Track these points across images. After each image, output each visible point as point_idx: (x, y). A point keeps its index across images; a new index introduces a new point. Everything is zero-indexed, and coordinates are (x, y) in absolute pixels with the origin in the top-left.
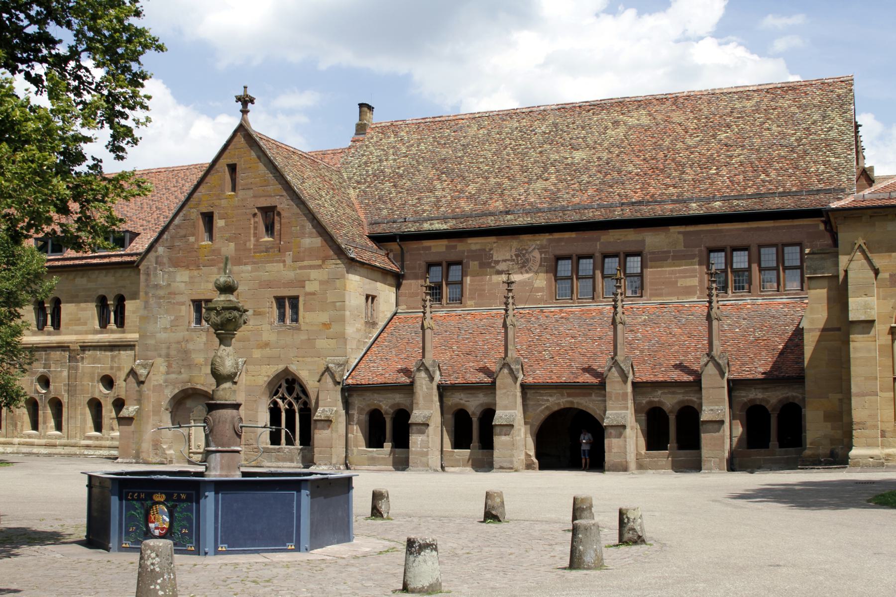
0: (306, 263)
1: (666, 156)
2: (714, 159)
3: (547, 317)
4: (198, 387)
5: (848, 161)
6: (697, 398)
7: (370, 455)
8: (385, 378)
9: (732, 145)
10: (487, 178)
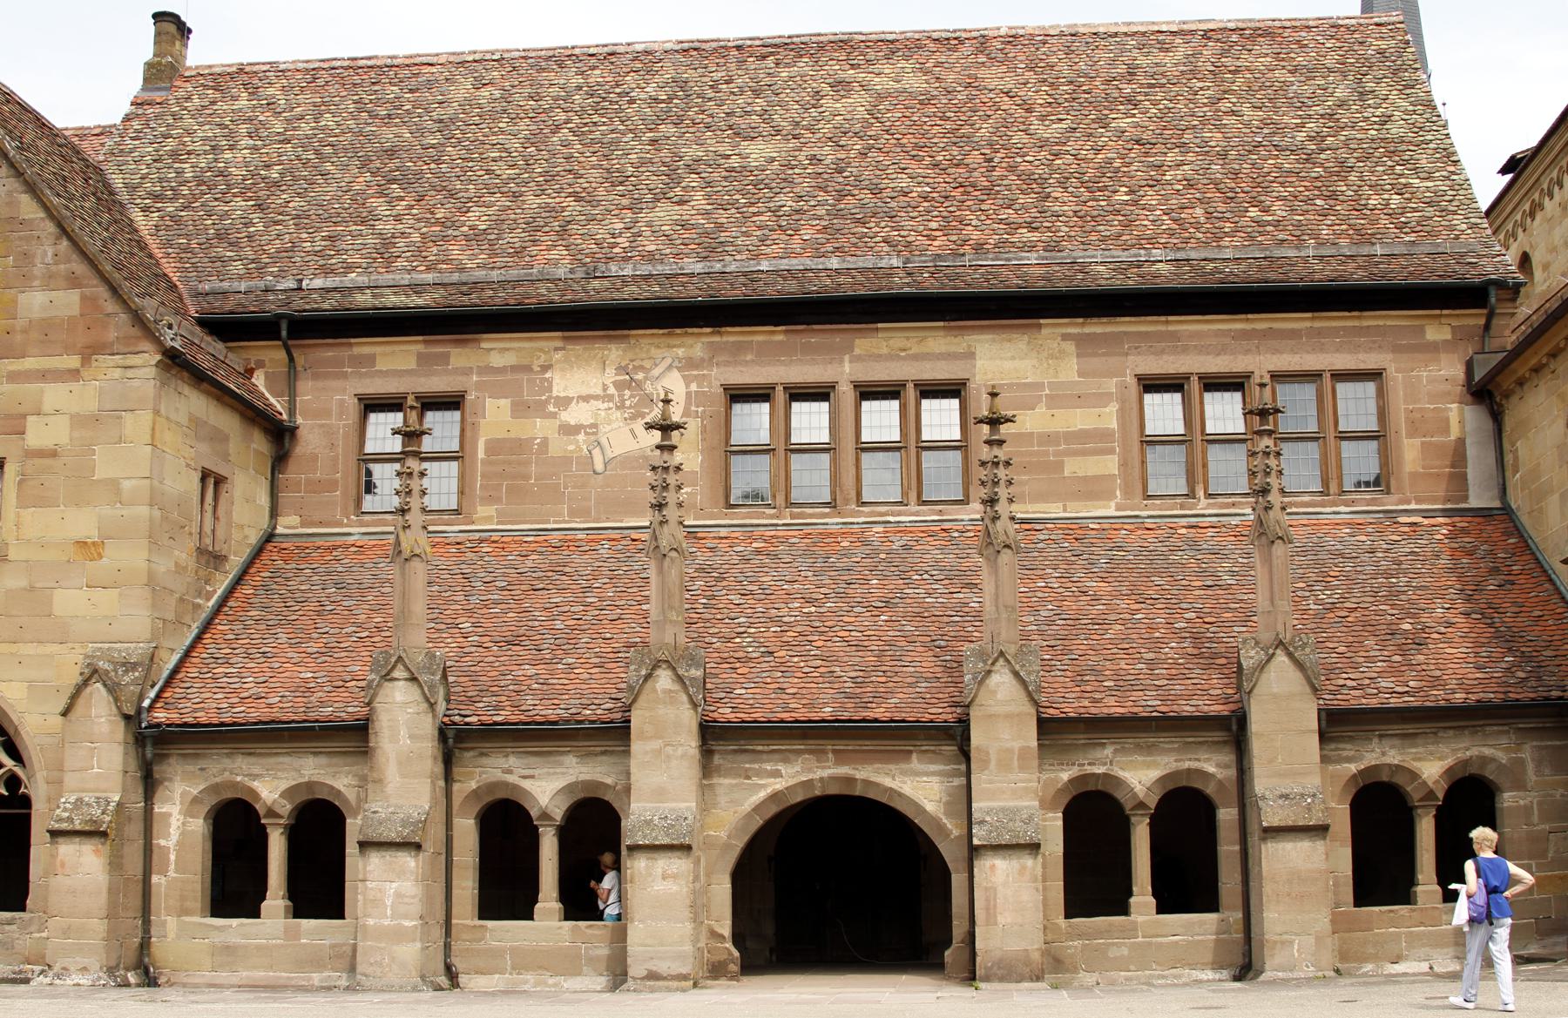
0: (30, 363)
1: (990, 160)
2: (1117, 170)
3: (711, 549)
5: (1457, 187)
6: (1218, 766)
7: (218, 938)
8: (270, 706)
9: (1154, 141)
10: (516, 196)
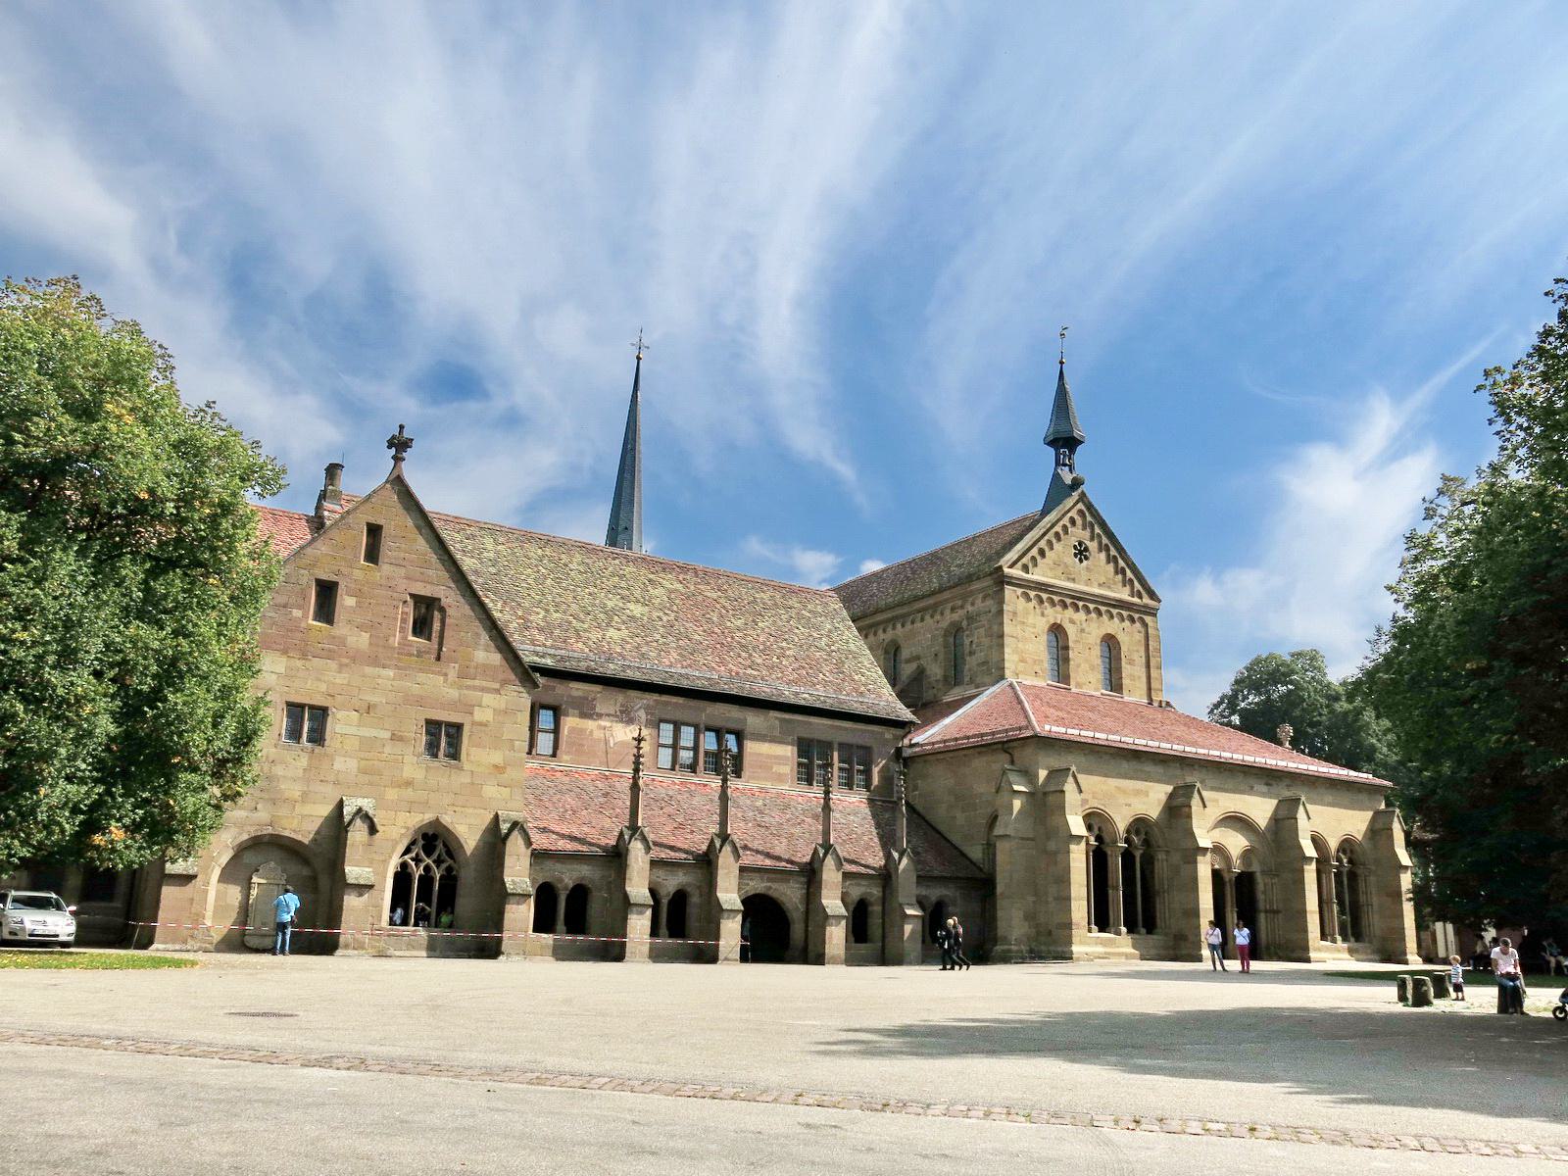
0: (477, 683)
4: (286, 833)
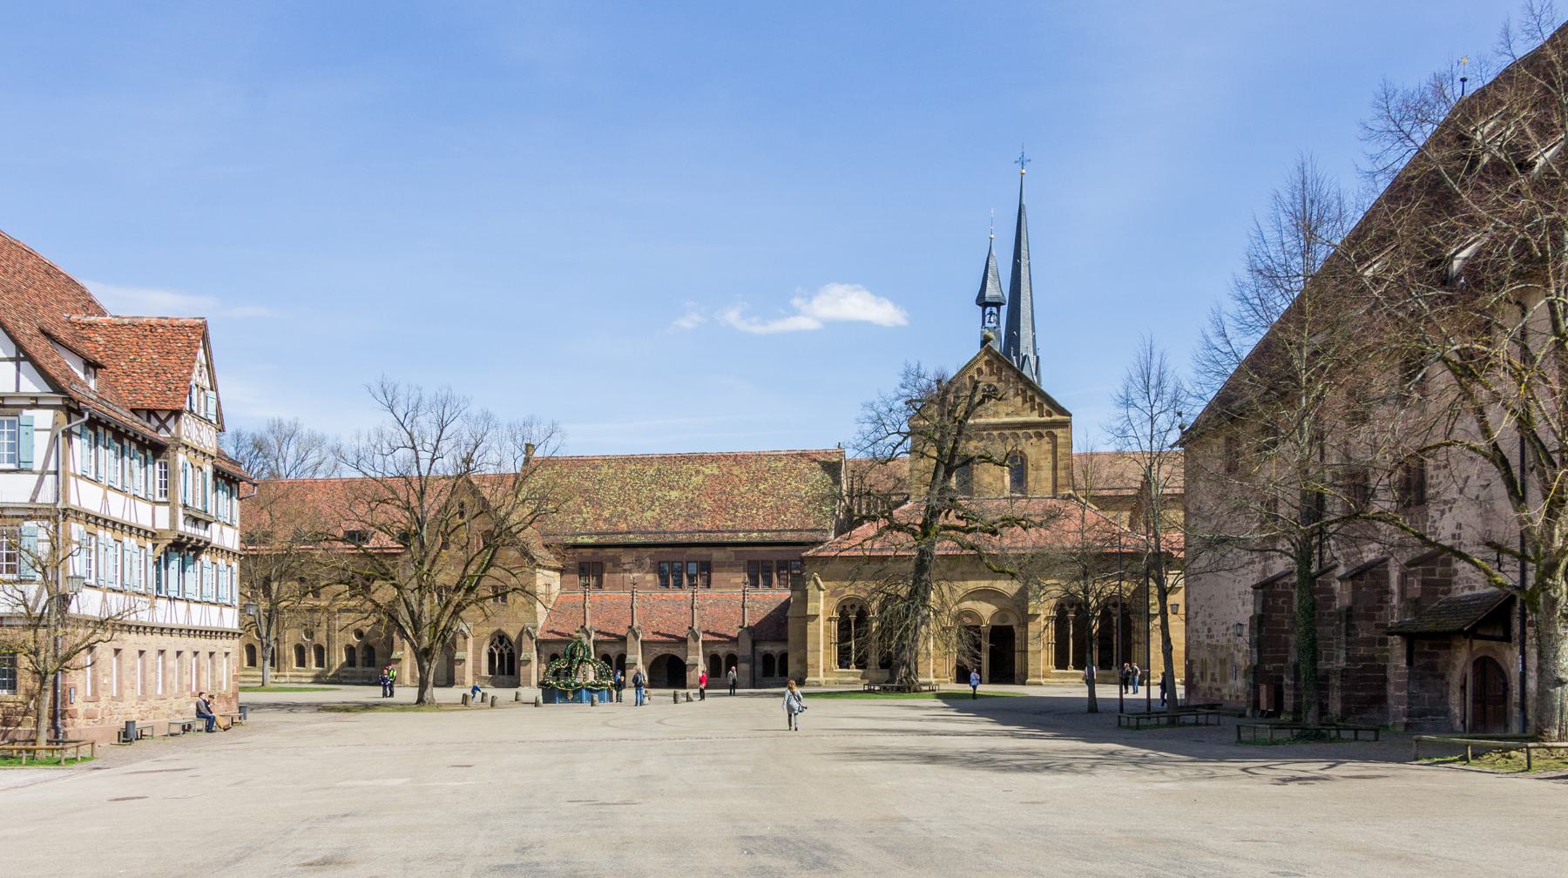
10: (616, 507)
